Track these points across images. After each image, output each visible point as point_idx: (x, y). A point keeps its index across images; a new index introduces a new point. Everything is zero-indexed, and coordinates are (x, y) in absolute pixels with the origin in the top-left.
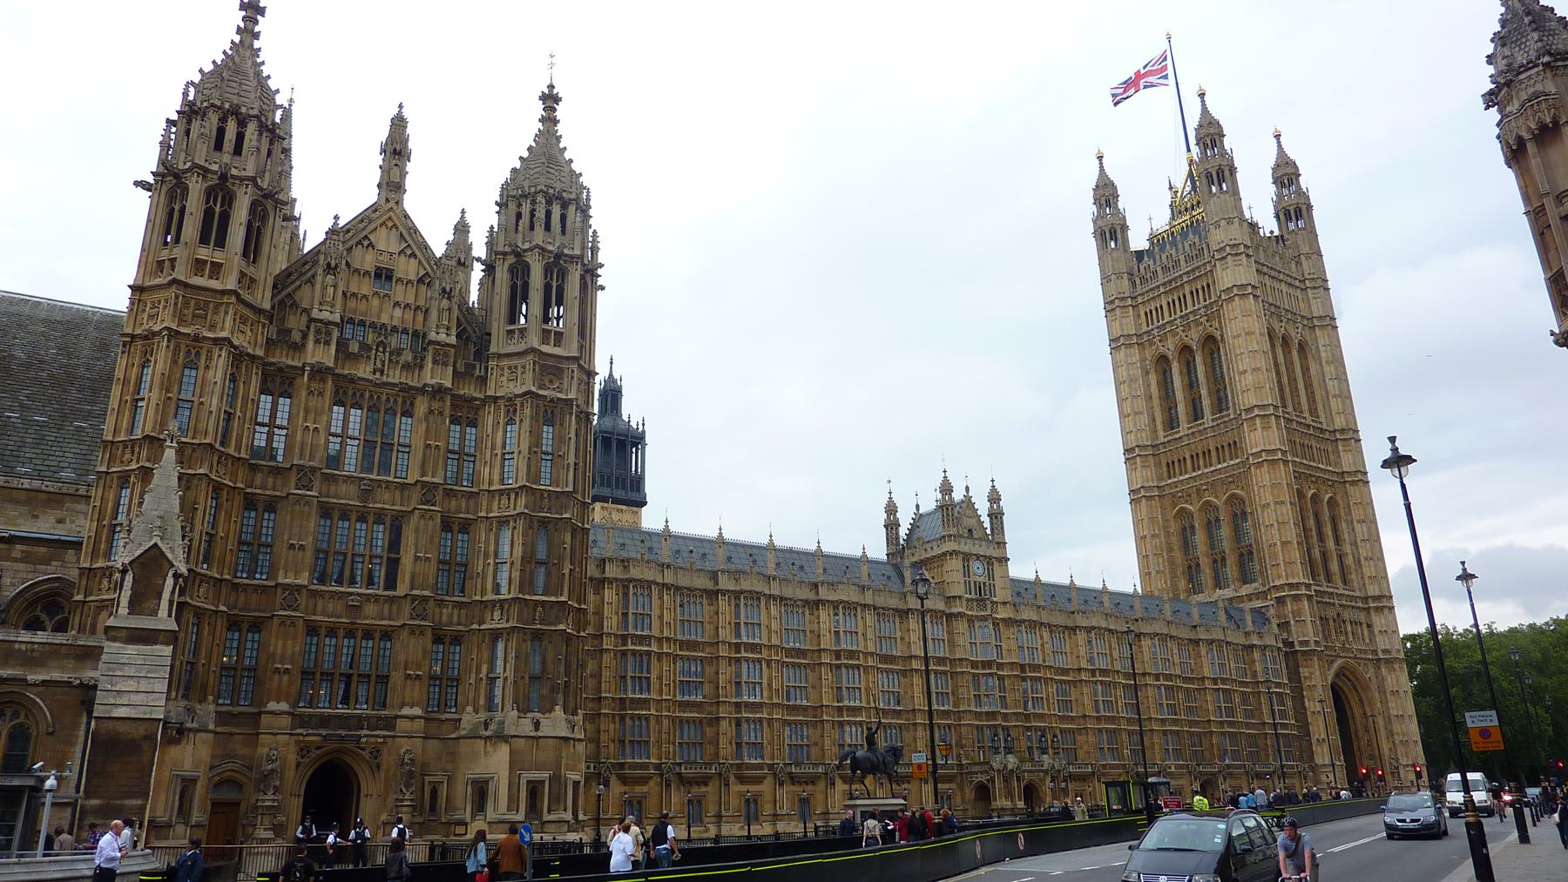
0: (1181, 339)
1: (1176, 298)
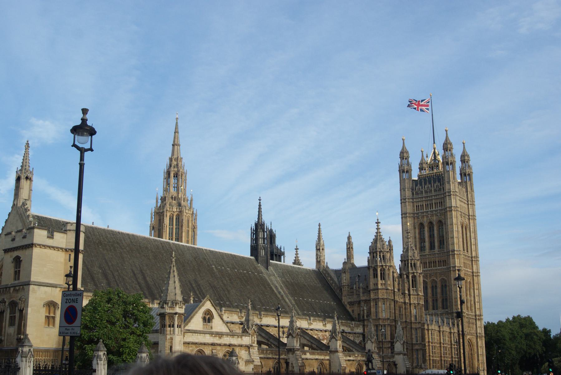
0: (430, 219)
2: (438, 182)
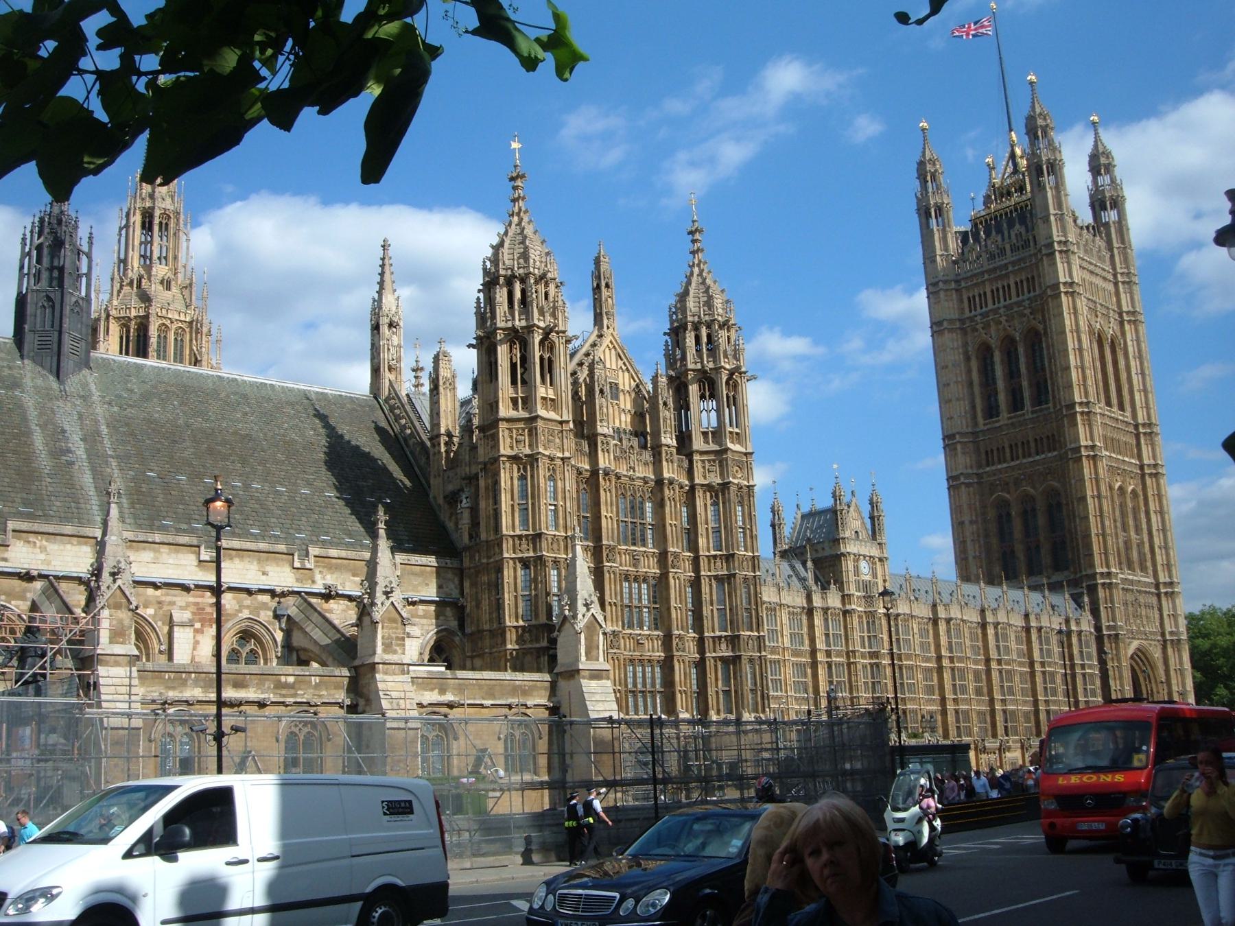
0: (1005, 329)
1: (1000, 286)
2: (1020, 224)
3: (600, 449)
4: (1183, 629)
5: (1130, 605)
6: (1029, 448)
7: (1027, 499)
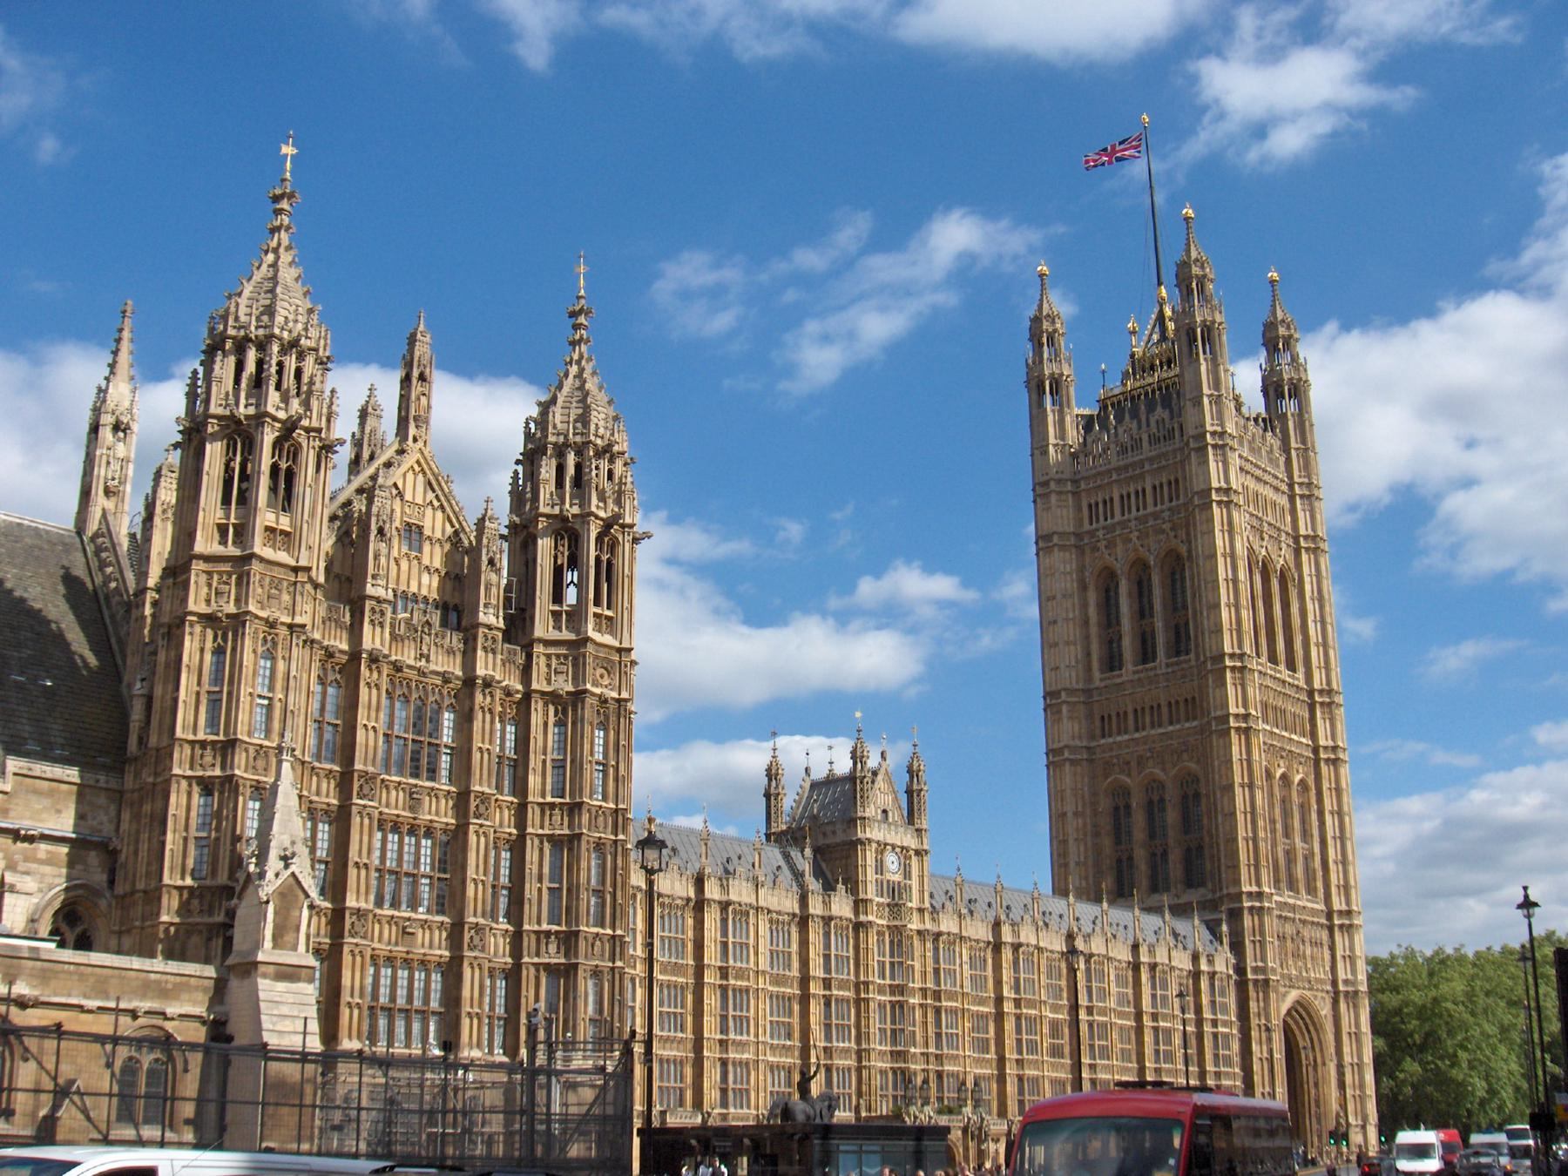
0: (1136, 550)
1: (1132, 490)
2: (1164, 407)
3: (367, 620)
4: (1362, 977)
5: (1289, 942)
6: (1160, 715)
7: (1154, 786)
